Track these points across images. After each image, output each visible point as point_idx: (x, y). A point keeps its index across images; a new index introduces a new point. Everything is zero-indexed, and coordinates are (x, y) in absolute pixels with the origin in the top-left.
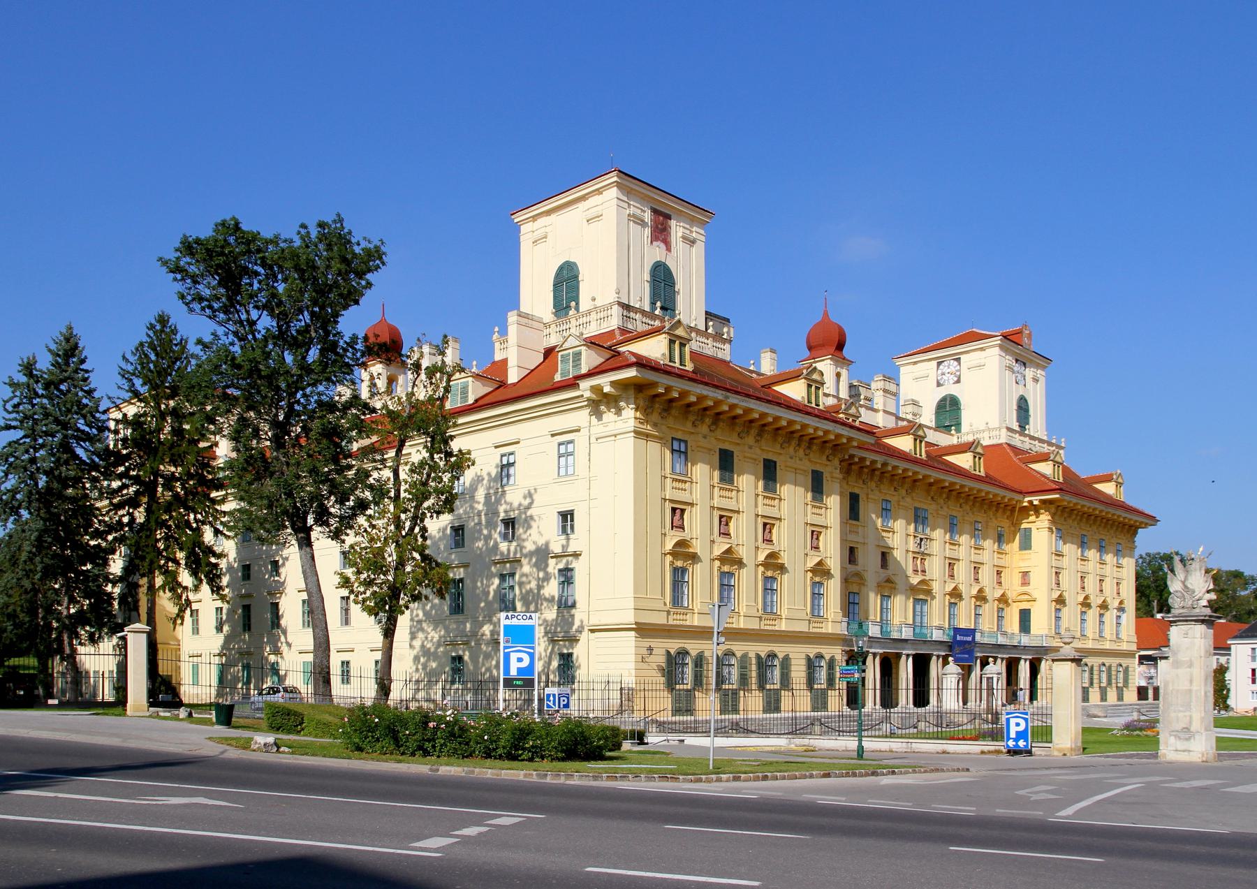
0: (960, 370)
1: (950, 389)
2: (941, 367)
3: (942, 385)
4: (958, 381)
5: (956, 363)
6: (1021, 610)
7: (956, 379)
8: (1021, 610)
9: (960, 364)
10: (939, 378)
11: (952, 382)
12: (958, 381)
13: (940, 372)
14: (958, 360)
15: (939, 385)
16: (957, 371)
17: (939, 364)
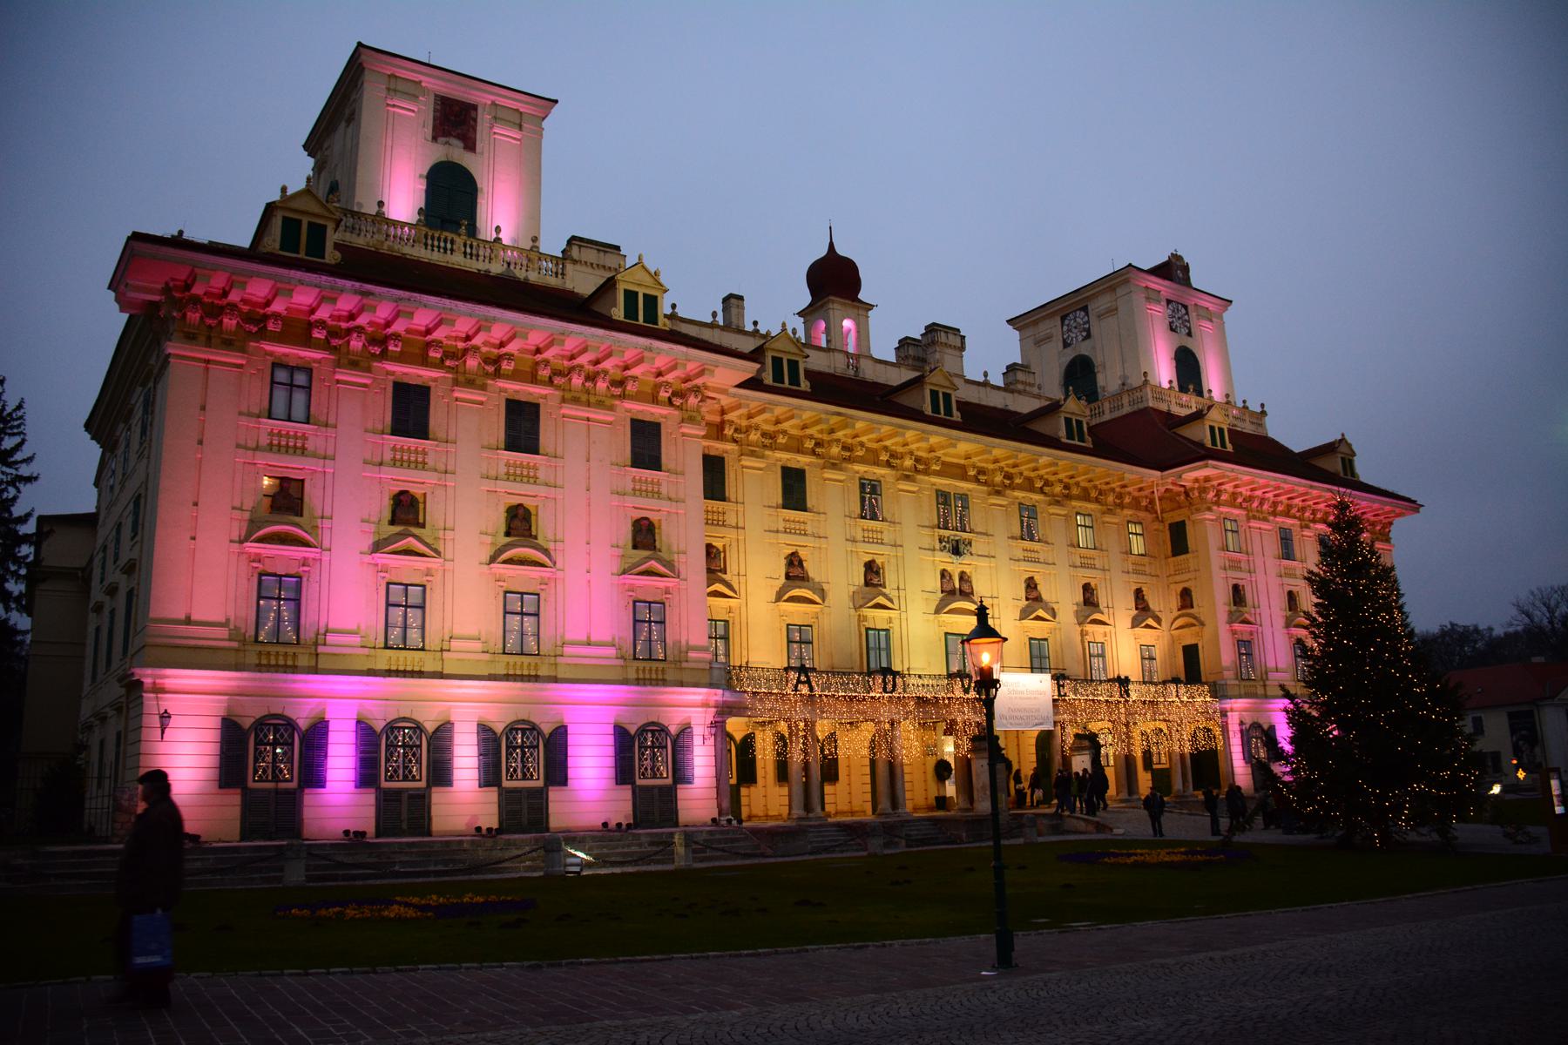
0: (1088, 322)
1: (1084, 349)
2: (1066, 322)
3: (1069, 345)
4: (1088, 336)
5: (1083, 313)
6: (1183, 647)
7: (1084, 334)
8: (1183, 647)
9: (1087, 314)
10: (1065, 337)
11: (1080, 338)
12: (1088, 336)
13: (1065, 328)
14: (1085, 309)
15: (1066, 345)
16: (1085, 323)
17: (1063, 319)
